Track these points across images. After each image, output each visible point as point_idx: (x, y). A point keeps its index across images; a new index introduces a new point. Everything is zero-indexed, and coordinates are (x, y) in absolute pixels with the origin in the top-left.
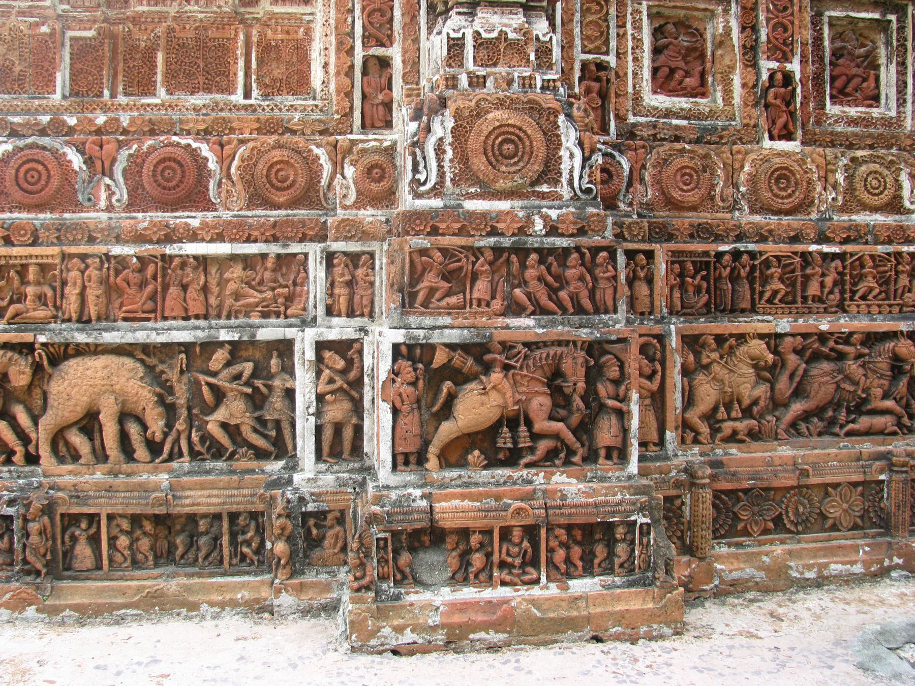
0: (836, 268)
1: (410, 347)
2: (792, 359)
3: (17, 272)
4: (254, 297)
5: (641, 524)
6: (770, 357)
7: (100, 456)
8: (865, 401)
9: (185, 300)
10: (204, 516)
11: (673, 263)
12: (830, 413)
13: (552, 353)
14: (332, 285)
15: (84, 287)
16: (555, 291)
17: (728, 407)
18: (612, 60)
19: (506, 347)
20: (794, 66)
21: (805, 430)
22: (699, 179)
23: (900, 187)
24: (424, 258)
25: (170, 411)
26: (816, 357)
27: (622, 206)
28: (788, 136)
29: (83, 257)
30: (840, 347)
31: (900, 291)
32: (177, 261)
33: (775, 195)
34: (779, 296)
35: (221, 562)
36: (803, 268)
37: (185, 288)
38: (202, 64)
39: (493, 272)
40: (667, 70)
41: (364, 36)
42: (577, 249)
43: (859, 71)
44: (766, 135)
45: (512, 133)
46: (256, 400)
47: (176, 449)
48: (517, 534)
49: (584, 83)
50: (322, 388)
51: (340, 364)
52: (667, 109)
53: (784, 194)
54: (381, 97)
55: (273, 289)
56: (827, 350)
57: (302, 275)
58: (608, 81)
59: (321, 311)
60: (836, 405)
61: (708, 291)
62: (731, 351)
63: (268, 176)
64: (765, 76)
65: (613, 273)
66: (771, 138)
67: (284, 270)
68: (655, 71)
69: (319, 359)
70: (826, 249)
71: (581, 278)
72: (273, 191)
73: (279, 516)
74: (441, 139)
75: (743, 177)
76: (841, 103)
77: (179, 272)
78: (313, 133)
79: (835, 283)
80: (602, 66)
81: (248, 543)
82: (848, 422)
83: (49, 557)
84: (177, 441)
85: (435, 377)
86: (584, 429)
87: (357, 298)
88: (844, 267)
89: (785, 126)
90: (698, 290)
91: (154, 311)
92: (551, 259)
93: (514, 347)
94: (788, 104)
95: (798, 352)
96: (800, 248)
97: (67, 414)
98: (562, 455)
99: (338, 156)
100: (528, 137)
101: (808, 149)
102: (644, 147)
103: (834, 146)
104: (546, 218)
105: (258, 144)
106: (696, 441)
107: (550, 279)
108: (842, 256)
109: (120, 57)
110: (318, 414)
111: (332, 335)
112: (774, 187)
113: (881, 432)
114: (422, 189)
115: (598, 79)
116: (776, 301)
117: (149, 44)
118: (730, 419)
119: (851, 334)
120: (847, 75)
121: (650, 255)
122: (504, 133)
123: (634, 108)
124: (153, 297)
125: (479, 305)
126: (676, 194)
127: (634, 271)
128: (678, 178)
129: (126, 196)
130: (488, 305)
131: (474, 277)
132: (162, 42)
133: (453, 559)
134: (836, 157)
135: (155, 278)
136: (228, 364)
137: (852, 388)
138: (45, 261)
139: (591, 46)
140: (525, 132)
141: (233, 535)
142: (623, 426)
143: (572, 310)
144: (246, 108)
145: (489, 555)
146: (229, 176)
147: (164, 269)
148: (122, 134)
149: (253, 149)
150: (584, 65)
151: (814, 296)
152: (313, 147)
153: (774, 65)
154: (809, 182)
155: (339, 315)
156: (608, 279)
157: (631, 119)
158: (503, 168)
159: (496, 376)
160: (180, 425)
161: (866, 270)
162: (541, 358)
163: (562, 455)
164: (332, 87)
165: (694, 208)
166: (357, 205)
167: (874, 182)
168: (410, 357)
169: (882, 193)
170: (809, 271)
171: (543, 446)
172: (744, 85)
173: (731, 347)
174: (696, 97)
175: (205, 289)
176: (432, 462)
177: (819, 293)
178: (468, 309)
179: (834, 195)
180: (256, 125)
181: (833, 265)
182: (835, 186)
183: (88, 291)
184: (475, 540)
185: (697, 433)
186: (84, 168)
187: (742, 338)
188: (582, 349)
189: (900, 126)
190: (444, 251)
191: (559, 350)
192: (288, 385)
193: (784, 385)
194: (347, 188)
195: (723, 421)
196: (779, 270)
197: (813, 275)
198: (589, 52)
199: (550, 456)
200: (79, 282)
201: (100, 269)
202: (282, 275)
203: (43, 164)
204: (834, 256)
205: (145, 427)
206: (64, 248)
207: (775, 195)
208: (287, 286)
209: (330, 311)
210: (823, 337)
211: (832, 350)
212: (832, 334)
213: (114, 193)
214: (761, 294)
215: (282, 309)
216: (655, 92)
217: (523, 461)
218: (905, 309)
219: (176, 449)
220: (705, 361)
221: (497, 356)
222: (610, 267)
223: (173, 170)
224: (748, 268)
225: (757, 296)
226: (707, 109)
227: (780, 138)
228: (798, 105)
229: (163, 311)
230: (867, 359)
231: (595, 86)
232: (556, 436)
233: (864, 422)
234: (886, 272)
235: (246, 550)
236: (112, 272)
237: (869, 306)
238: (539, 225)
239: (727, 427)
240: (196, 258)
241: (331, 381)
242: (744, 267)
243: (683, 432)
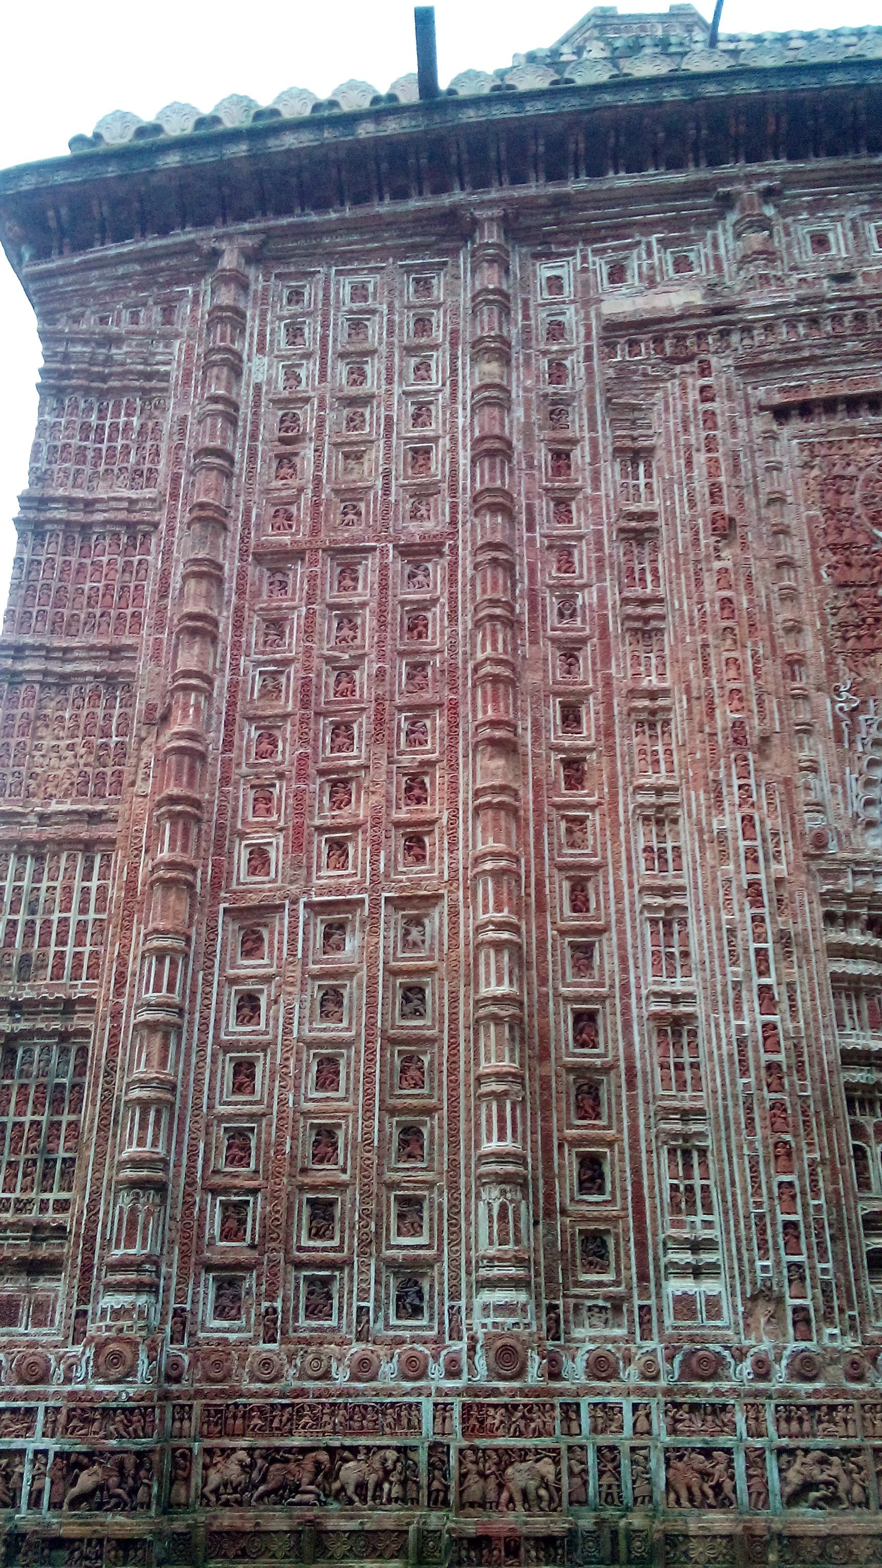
2: (260, 1462)
6: (248, 1460)
17: (225, 1486)
18: (188, 1307)
19: (101, 1454)
20: (278, 1305)
26: (274, 1461)
60: (283, 1486)
62: (228, 1457)
70: (284, 1401)
79: (289, 1420)
80: (183, 1310)
85: (71, 1467)
86: (133, 1492)
99: (60, 1359)
108: (292, 1405)
113: (307, 1504)
121: (191, 1406)
131: (94, 1420)
150: (175, 1310)
153: (267, 1304)
166: (63, 1383)
171: (113, 1501)
176: (65, 1507)
187: (234, 1450)
190: (83, 1410)
199: (117, 1505)
204: (287, 1405)
232: (119, 1496)
233: (298, 1498)
238: (124, 1396)
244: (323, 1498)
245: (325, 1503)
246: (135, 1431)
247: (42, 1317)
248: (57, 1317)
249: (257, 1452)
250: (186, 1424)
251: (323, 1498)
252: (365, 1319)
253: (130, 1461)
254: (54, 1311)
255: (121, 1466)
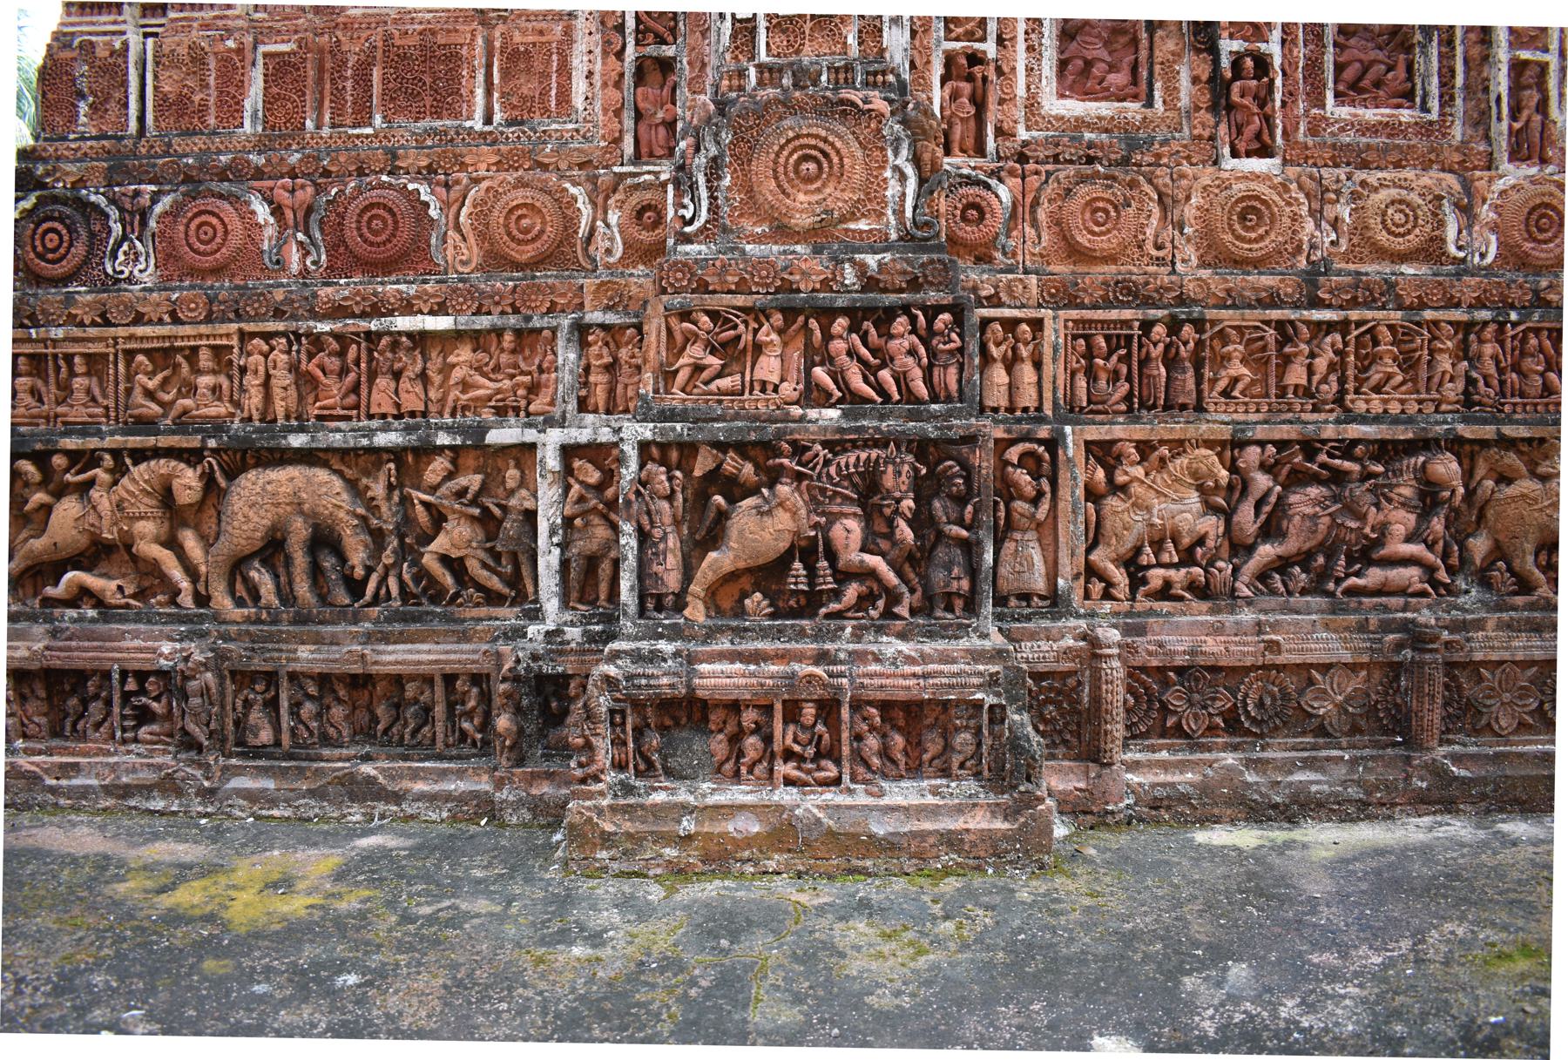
0: (1333, 345)
1: (664, 447)
3: (185, 357)
4: (485, 387)
5: (991, 707)
7: (286, 596)
8: (1379, 542)
9: (396, 392)
10: (412, 678)
11: (1075, 337)
12: (1321, 560)
13: (864, 455)
14: (587, 369)
15: (268, 376)
16: (874, 371)
17: (1158, 546)
21: (1279, 585)
22: (1118, 217)
23: (1441, 224)
24: (685, 325)
25: (378, 537)
26: (1298, 479)
27: (998, 255)
28: (1265, 151)
29: (267, 336)
30: (1338, 462)
31: (1436, 380)
32: (385, 341)
33: (1238, 238)
34: (1240, 386)
35: (434, 740)
36: (1280, 345)
37: (397, 375)
38: (428, 80)
39: (785, 344)
40: (1080, 63)
41: (637, 31)
42: (906, 309)
43: (1381, 55)
44: (1227, 151)
45: (815, 147)
46: (488, 523)
47: (383, 591)
48: (809, 711)
49: (949, 84)
50: (568, 511)
51: (594, 476)
52: (1077, 119)
53: (1253, 235)
54: (660, 115)
55: (512, 377)
56: (1315, 467)
57: (550, 357)
58: (985, 79)
59: (572, 406)
60: (1330, 550)
61: (1129, 379)
63: (506, 226)
64: (1225, 62)
65: (959, 343)
66: (1235, 154)
67: (527, 352)
68: (1062, 65)
69: (568, 470)
71: (912, 352)
72: (513, 245)
73: (504, 680)
74: (714, 159)
75: (1190, 212)
76: (1352, 104)
77: (389, 355)
78: (570, 168)
79: (1332, 367)
80: (975, 59)
81: (469, 715)
82: (1348, 576)
83: (213, 726)
84: (383, 580)
87: (620, 388)
88: (1346, 344)
89: (1258, 136)
90: (1114, 377)
91: (357, 407)
92: (867, 325)
93: (809, 449)
94: (1262, 106)
95: (1264, 467)
96: (1275, 314)
97: (243, 542)
98: (881, 603)
100: (838, 152)
101: (1292, 171)
102: (1037, 173)
103: (1336, 166)
104: (861, 268)
105: (494, 184)
106: (1107, 596)
107: (864, 351)
108: (1343, 326)
109: (327, 76)
110: (564, 546)
111: (583, 436)
112: (1237, 226)
113: (1402, 592)
114: (688, 229)
115: (970, 78)
116: (1236, 393)
117: (363, 57)
118: (1160, 565)
119: (1355, 442)
120: (1361, 61)
121: (1037, 325)
122: (802, 147)
123: (1027, 120)
124: (355, 389)
125: (763, 391)
126: (1083, 239)
127: (1014, 349)
128: (1088, 215)
129: (324, 257)
130: (776, 389)
131: (758, 349)
132: (379, 54)
133: (719, 745)
134: (1338, 181)
135: (357, 363)
136: (450, 476)
137: (1353, 524)
138: (218, 342)
139: (960, 30)
140: (832, 145)
141: (451, 707)
142: (971, 565)
143: (897, 397)
144: (483, 135)
145: (768, 740)
146: (457, 227)
147: (370, 351)
148: (321, 175)
149: (488, 190)
150: (950, 59)
151: (1297, 386)
152: (567, 185)
154: (1295, 218)
155: (595, 411)
156: (950, 352)
157: (1023, 134)
158: (801, 197)
159: (784, 489)
160: (388, 558)
161: (1382, 348)
162: (847, 466)
163: (881, 603)
164: (598, 106)
165: (1111, 259)
167: (1399, 218)
168: (663, 462)
169: (1409, 232)
170: (1287, 350)
171: (852, 592)
172: (1195, 80)
173: (1162, 460)
174: (1124, 100)
175: (423, 377)
177: (1304, 382)
178: (747, 395)
179: (1333, 236)
180: (495, 159)
181: (1328, 339)
182: (1335, 223)
183: (273, 381)
184: (749, 717)
185: (1109, 584)
186: (271, 220)
187: (1179, 446)
188: (909, 451)
189: (1444, 135)
191: (874, 453)
192: (528, 505)
193: (1247, 519)
194: (612, 239)
195: (1149, 567)
196: (1241, 348)
197: (1296, 355)
198: (957, 39)
200: (261, 369)
201: (289, 352)
202: (525, 359)
203: (218, 217)
204: (1330, 327)
205: (342, 559)
206: (242, 325)
207: (1238, 238)
208: (530, 373)
209: (583, 406)
210: (1309, 447)
211: (1323, 466)
212: (1324, 442)
213: (308, 253)
214: (1213, 381)
215: (523, 403)
216: (1062, 96)
217: (823, 610)
218: (1444, 407)
219: (383, 591)
220: (1121, 478)
221: (786, 461)
222: (954, 336)
223: (384, 221)
224: (1192, 344)
225: (1205, 386)
226: (1139, 117)
227: (1249, 155)
228: (1278, 104)
229: (368, 406)
230: (1381, 480)
231: (966, 87)
233: (1374, 576)
234: (1415, 351)
235: (466, 725)
236: (304, 357)
237: (1385, 402)
239: (1156, 576)
240: (410, 335)
241: (581, 499)
242: (1185, 343)
243: (1087, 582)
244: (1443, 575)
245: (1450, 590)
246: (901, 379)
247: (529, 87)
248: (579, 87)
249: (1253, 452)
250: (1027, 373)
251: (1443, 575)
252: (1531, 97)
253: (898, 478)
254: (565, 70)
255: (868, 490)
